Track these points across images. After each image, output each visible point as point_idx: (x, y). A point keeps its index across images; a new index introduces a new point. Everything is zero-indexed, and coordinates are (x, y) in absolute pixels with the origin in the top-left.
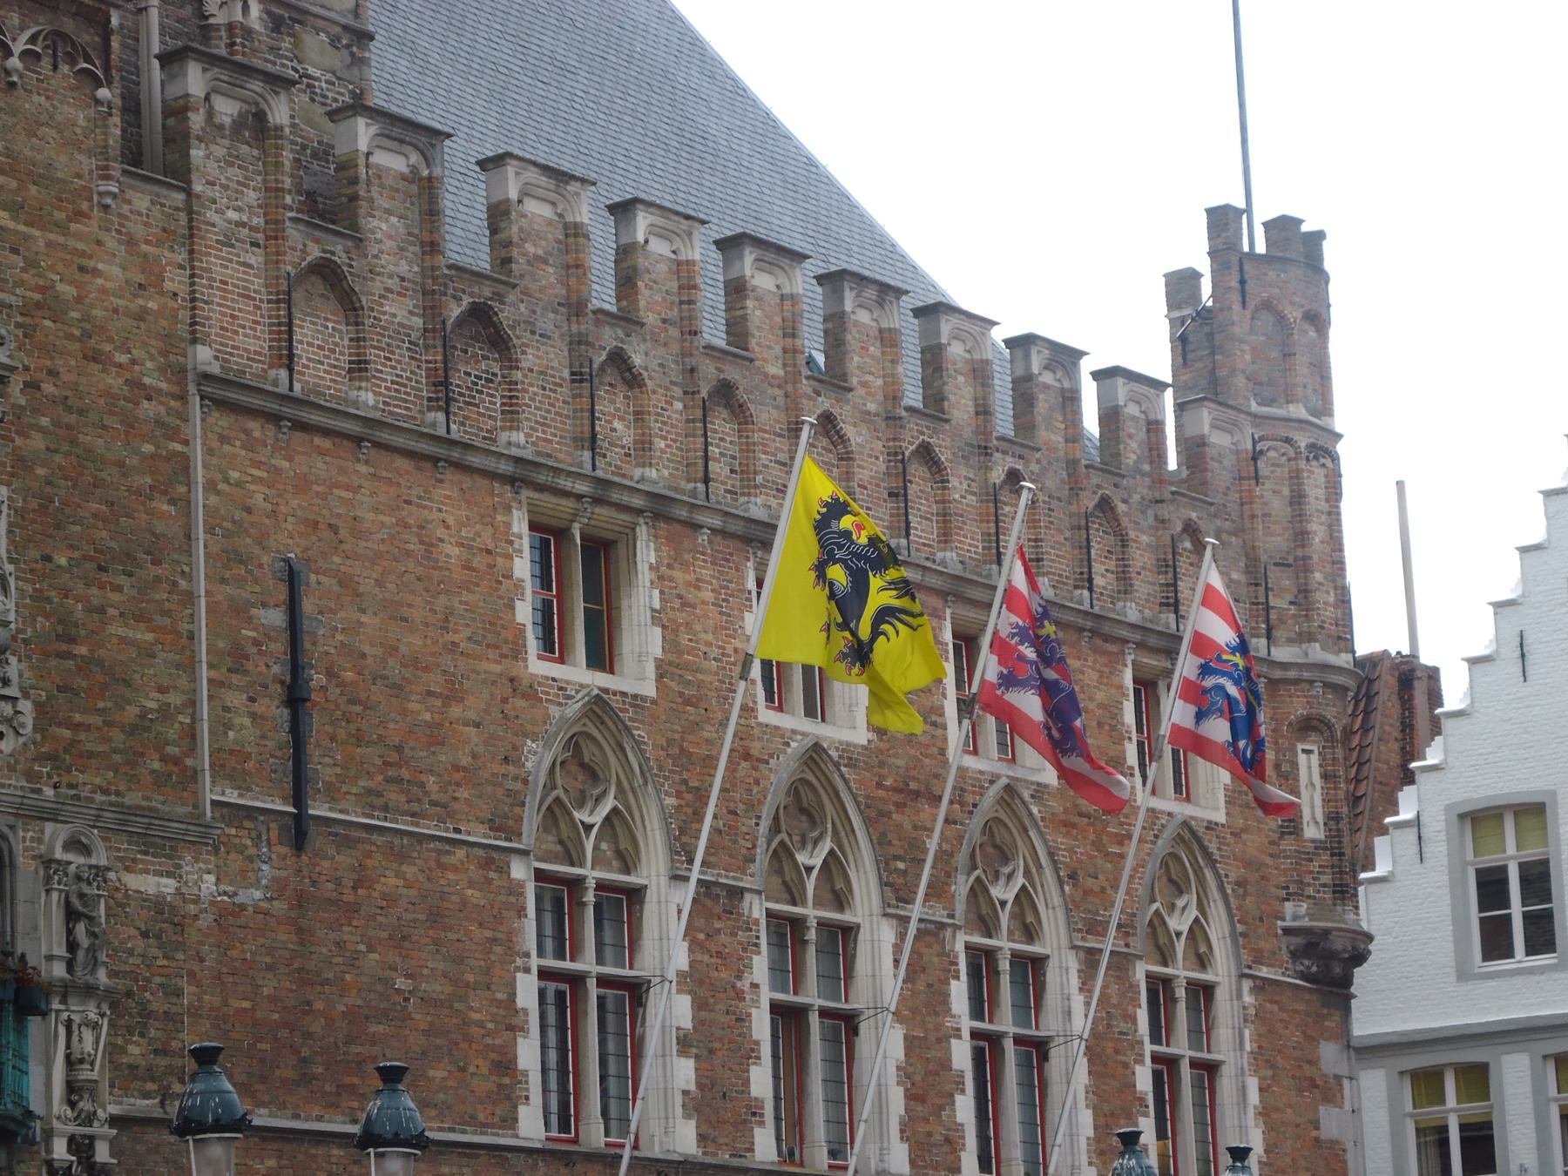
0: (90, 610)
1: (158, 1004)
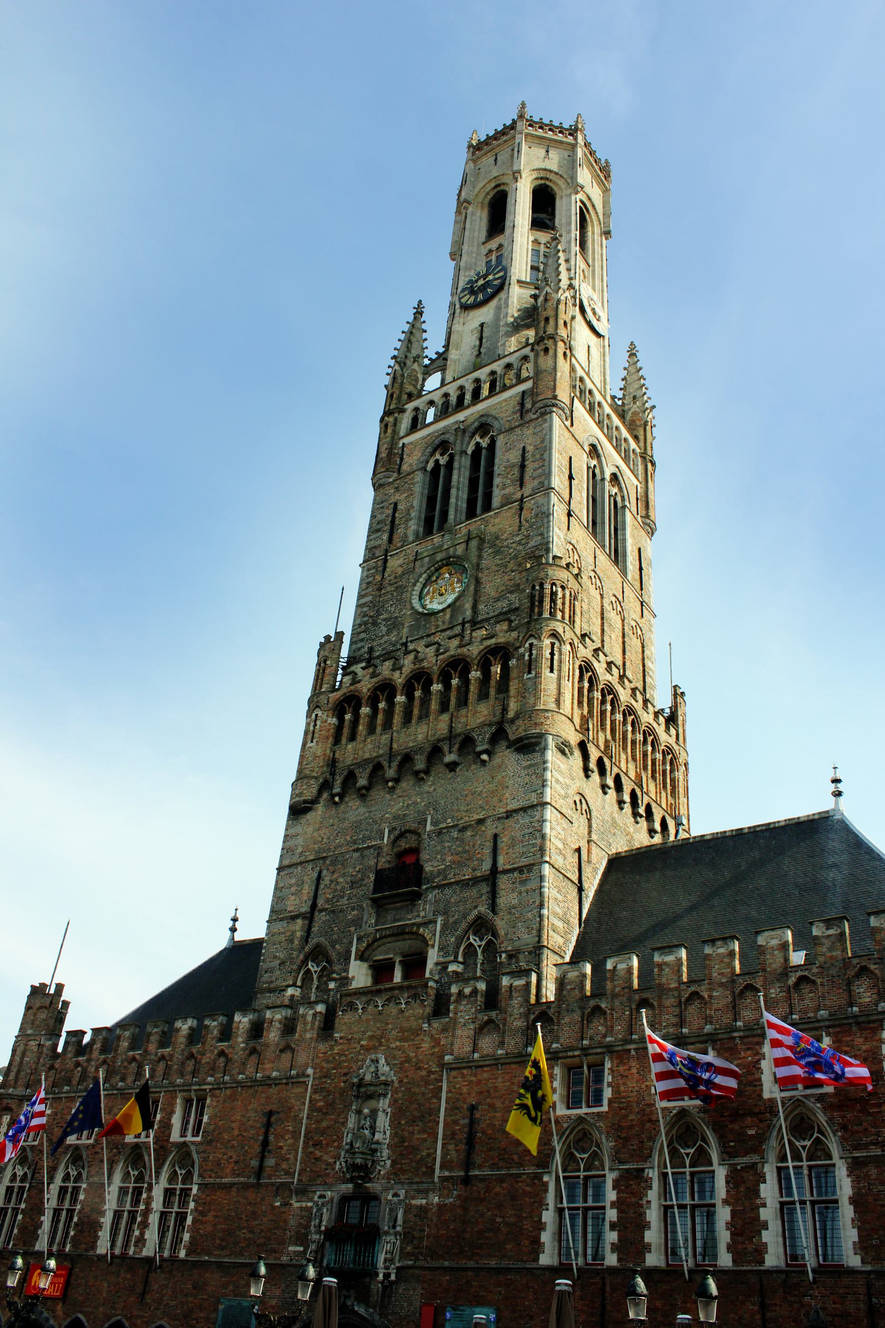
0: (409, 1133)
1: (416, 1234)
